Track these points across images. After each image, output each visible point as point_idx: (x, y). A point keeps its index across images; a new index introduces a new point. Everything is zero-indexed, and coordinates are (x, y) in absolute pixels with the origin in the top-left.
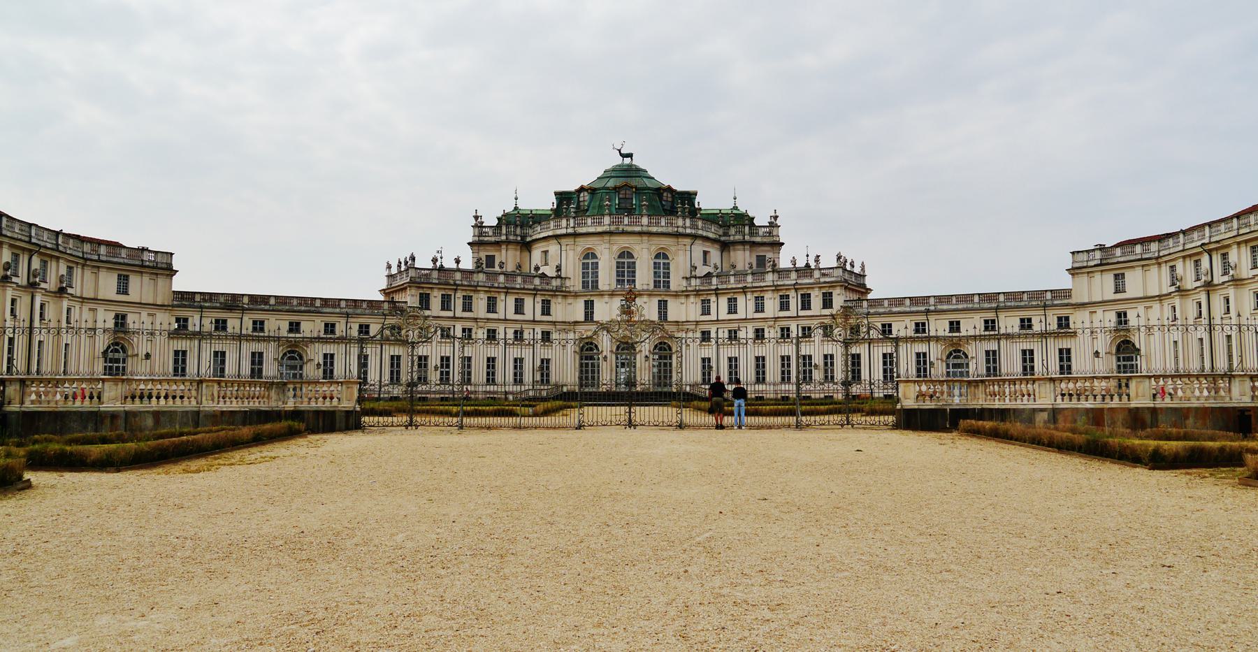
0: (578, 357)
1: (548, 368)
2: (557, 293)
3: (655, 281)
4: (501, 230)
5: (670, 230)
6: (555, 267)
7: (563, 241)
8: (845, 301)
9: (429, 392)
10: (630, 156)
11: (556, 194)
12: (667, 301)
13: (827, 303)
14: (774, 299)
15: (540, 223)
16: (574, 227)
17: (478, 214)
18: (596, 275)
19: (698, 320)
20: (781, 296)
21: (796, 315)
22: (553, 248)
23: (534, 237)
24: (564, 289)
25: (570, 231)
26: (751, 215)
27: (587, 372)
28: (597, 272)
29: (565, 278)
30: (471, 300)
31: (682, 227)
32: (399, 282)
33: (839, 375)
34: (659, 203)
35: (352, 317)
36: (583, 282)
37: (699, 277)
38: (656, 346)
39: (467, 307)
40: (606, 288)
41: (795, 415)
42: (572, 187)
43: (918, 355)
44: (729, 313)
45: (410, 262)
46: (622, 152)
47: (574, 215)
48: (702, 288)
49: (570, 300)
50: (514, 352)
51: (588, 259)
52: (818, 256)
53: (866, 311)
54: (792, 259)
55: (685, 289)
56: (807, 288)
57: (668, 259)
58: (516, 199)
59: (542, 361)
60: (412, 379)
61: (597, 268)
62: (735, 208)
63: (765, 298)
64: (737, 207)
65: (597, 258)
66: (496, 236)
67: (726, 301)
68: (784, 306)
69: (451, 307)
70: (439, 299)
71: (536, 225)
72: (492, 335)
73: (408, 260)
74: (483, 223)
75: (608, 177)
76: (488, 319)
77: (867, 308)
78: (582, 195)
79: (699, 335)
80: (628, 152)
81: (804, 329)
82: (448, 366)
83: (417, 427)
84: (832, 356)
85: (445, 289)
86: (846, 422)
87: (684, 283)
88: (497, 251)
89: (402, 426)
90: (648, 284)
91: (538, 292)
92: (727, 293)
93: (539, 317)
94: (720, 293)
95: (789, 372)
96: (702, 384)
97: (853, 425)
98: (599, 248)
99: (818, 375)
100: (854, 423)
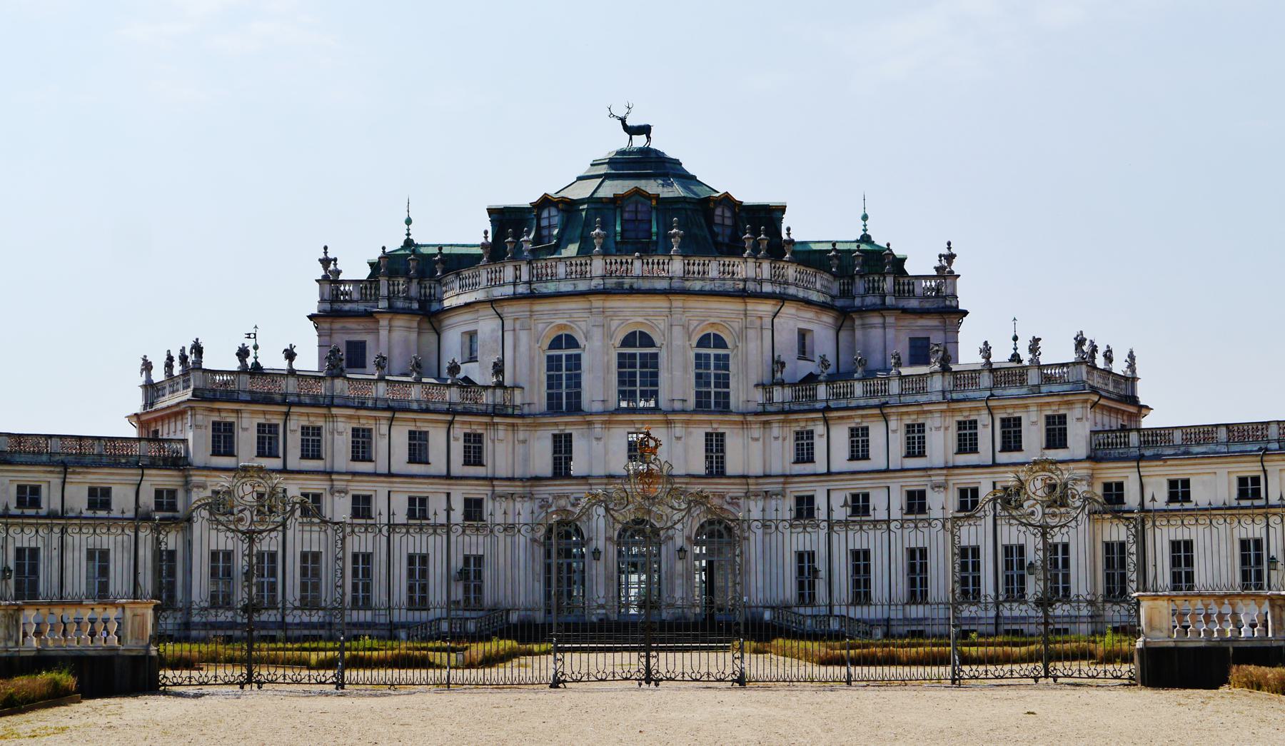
1: (479, 575)
2: (496, 420)
3: (698, 394)
4: (377, 289)
5: (729, 285)
7: (509, 310)
8: (1093, 432)
10: (645, 130)
11: (491, 212)
12: (723, 435)
13: (1056, 435)
14: (946, 429)
15: (458, 275)
16: (529, 283)
17: (330, 256)
18: (575, 381)
19: (788, 472)
20: (959, 423)
21: (991, 463)
22: (487, 326)
23: (447, 304)
24: (510, 411)
25: (522, 289)
26: (898, 252)
28: (579, 376)
29: (513, 388)
30: (319, 434)
32: (167, 401)
33: (1034, 587)
34: (706, 230)
35: (74, 473)
36: (550, 396)
37: (792, 385)
38: (702, 526)
39: (312, 448)
40: (597, 407)
41: (948, 663)
42: (524, 197)
43: (1244, 544)
44: (853, 457)
45: (192, 358)
46: (629, 123)
47: (530, 257)
48: (796, 408)
50: (407, 544)
51: (561, 348)
52: (1036, 341)
53: (1135, 452)
54: (982, 346)
55: (760, 409)
56: (1015, 406)
59: (466, 559)
60: (250, 598)
61: (578, 366)
62: (866, 239)
63: (927, 428)
64: (869, 237)
65: (577, 346)
66: (366, 301)
68: (967, 443)
70: (253, 434)
71: (451, 277)
73: (187, 353)
74: (339, 272)
76: (354, 474)
77: (1139, 447)
78: (545, 214)
80: (642, 123)
82: (273, 573)
83: (260, 684)
85: (264, 413)
86: (1043, 673)
87: (759, 396)
88: (369, 331)
89: (232, 683)
90: (684, 401)
91: (457, 418)
92: (849, 417)
93: (458, 468)
94: (832, 418)
95: (977, 581)
96: (798, 606)
97: (1055, 678)
98: (583, 325)
100: (1059, 674)
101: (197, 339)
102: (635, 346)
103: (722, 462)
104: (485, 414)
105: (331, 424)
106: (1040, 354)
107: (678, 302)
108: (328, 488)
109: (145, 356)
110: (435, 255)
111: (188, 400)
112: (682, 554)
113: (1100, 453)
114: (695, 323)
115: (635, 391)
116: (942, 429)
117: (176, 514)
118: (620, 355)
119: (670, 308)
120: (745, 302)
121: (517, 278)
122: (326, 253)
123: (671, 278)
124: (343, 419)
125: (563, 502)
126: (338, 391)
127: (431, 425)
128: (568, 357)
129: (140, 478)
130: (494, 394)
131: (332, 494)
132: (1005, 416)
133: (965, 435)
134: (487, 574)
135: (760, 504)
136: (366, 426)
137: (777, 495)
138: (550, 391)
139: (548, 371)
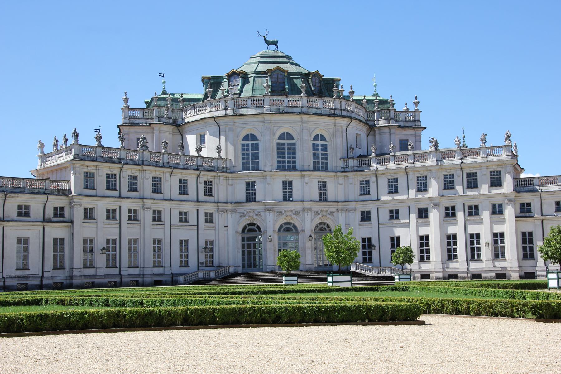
0: (240, 238)
1: (211, 250)
2: (220, 174)
3: (314, 163)
5: (327, 112)
6: (217, 148)
9: (95, 276)
10: (275, 43)
11: (203, 79)
12: (325, 182)
14: (438, 178)
17: (128, 96)
23: (186, 121)
25: (229, 112)
27: (249, 253)
28: (258, 153)
30: (136, 180)
31: (339, 109)
35: (10, 197)
36: (243, 163)
38: (317, 226)
39: (133, 188)
42: (221, 72)
46: (267, 39)
48: (360, 169)
49: (230, 182)
50: (181, 233)
55: (343, 170)
57: (325, 140)
58: (164, 83)
59: (206, 242)
61: (257, 149)
62: (377, 95)
65: (256, 139)
67: (387, 181)
69: (115, 186)
72: (157, 217)
75: (256, 63)
76: (154, 199)
79: (358, 216)
81: (470, 207)
82: (114, 249)
84: (531, 234)
87: (341, 164)
95: (455, 250)
99: (486, 252)
101: (76, 129)
102: (284, 139)
103: (326, 195)
104: (214, 171)
105: (142, 174)
106: (486, 142)
107: (305, 117)
108: (141, 206)
109: (40, 140)
110: (180, 98)
111: (72, 160)
112: (311, 238)
113: (518, 189)
114: (313, 129)
115: (285, 161)
116: (437, 178)
117: (65, 219)
118: (278, 144)
119: (302, 121)
120: (335, 120)
121: (226, 107)
122: (126, 95)
123: (302, 107)
124: (148, 172)
125: (251, 214)
126: (146, 158)
127: (189, 176)
128: (252, 145)
129: (46, 200)
130: (217, 162)
131: (144, 210)
132: (468, 172)
133: (448, 181)
134: (216, 249)
135: (344, 215)
136: (159, 176)
137: (352, 210)
138: (243, 161)
139: (242, 151)
